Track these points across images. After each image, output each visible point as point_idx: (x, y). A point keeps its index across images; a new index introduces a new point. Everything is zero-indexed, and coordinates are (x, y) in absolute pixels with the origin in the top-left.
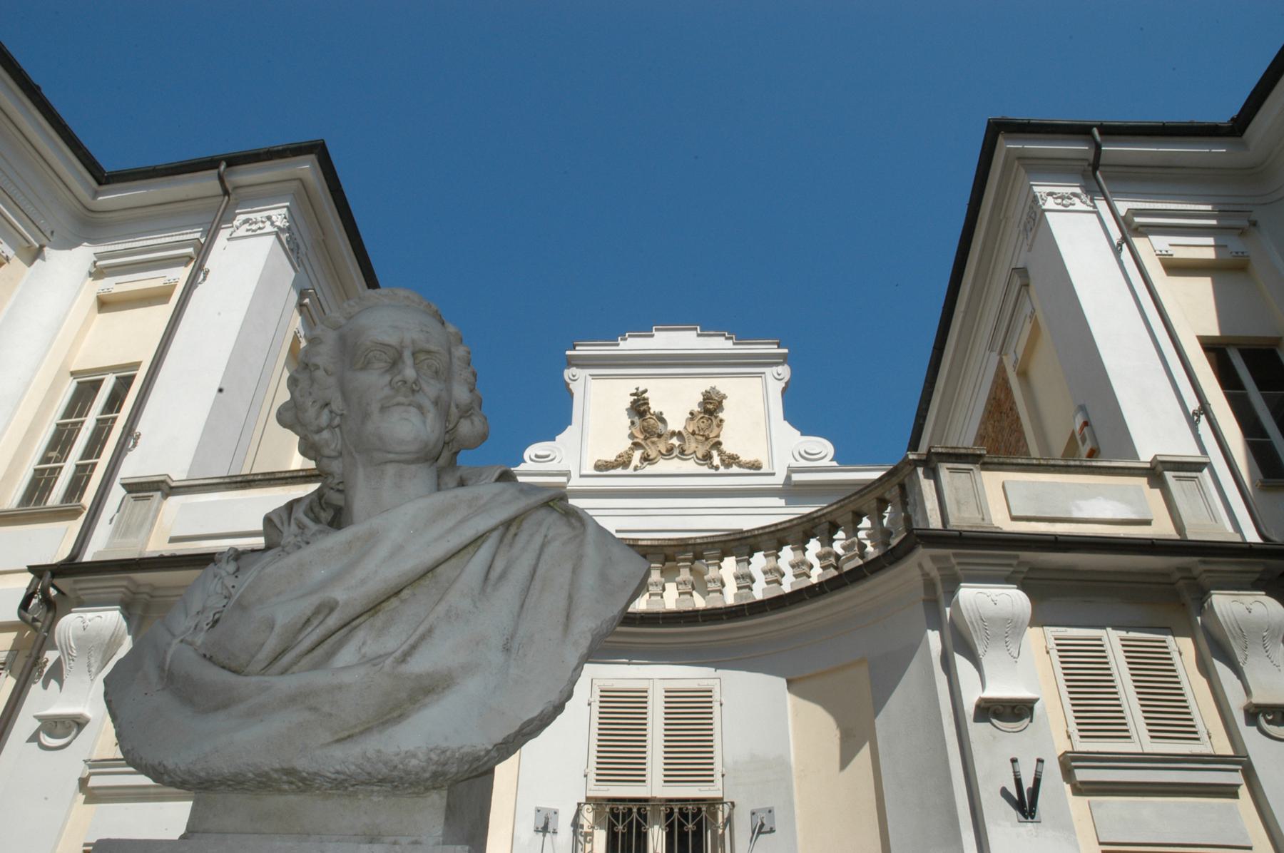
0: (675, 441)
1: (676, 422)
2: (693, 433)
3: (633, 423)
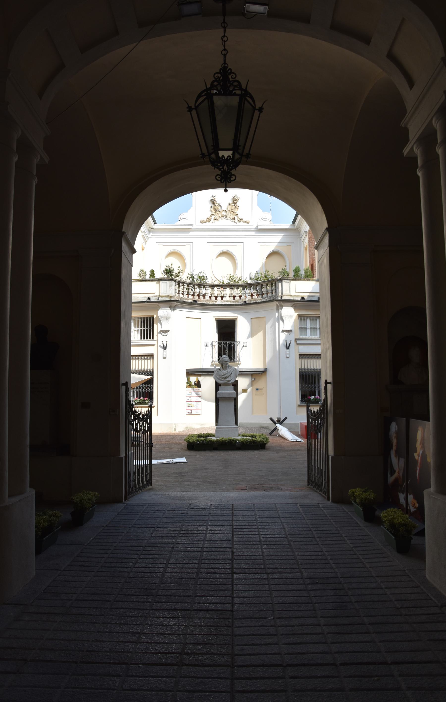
0: (224, 213)
2: (230, 211)
3: (211, 207)
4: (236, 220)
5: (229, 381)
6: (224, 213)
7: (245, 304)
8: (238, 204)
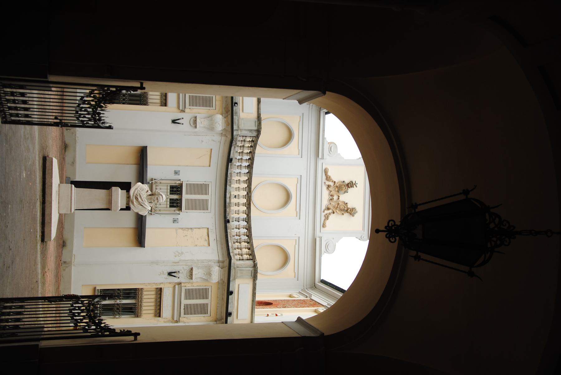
1: (344, 198)
2: (338, 204)
4: (327, 212)
5: (133, 203)
6: (335, 198)
7: (227, 221)
8: (346, 215)
